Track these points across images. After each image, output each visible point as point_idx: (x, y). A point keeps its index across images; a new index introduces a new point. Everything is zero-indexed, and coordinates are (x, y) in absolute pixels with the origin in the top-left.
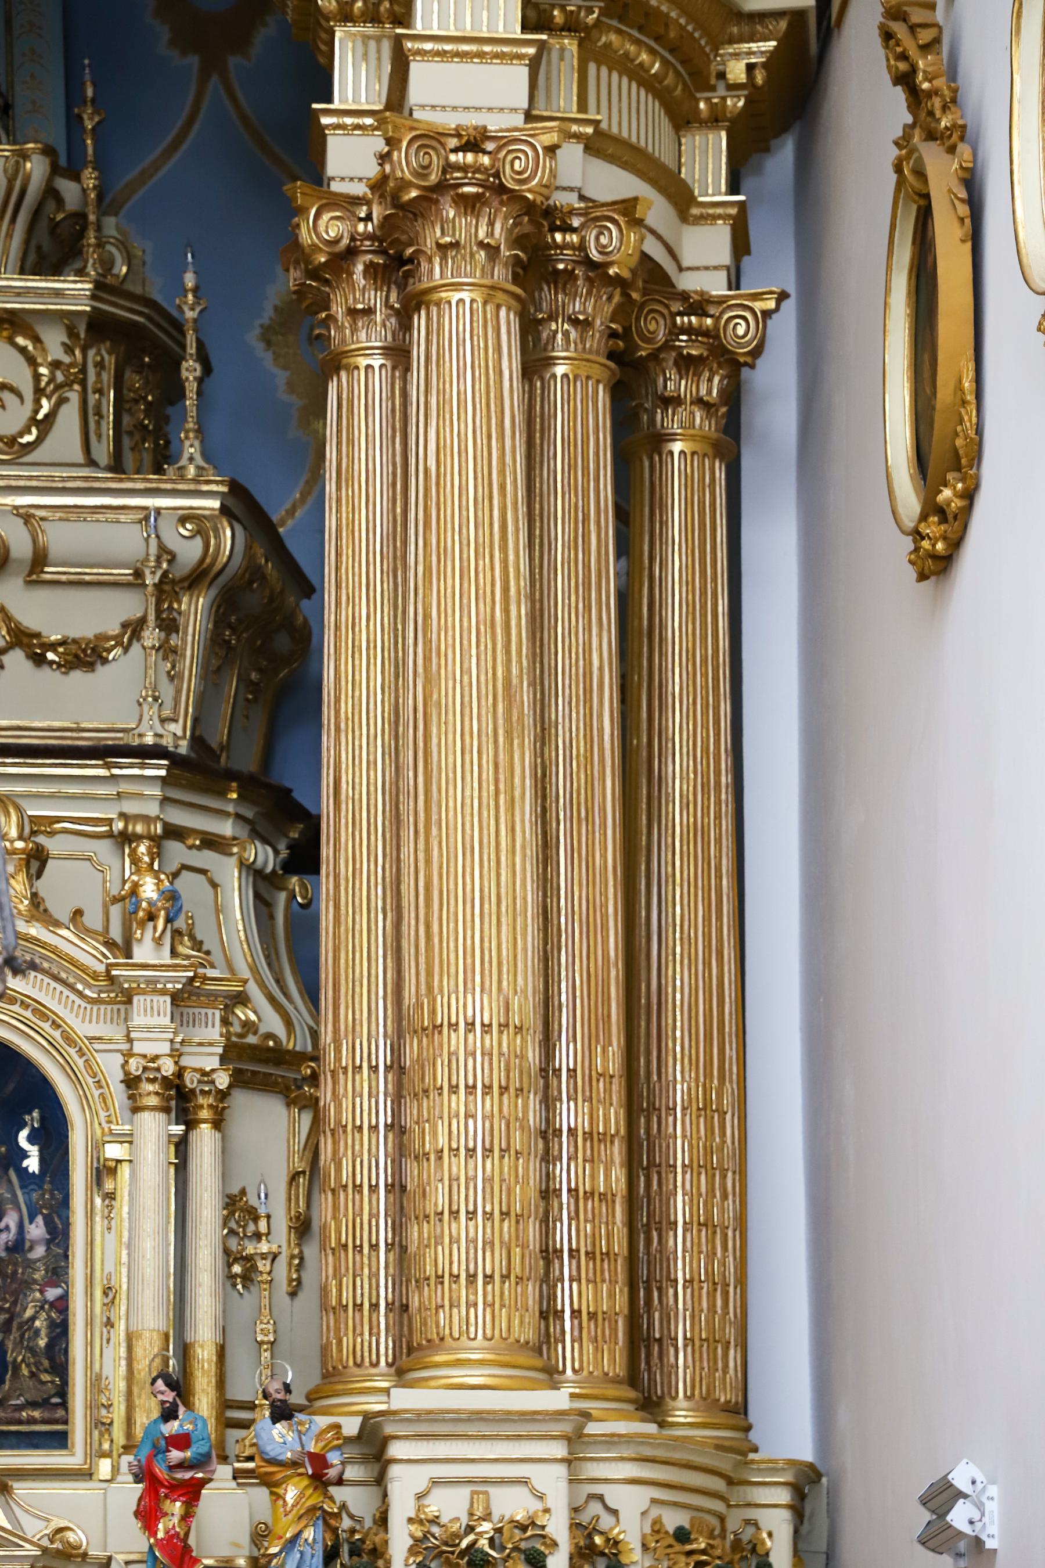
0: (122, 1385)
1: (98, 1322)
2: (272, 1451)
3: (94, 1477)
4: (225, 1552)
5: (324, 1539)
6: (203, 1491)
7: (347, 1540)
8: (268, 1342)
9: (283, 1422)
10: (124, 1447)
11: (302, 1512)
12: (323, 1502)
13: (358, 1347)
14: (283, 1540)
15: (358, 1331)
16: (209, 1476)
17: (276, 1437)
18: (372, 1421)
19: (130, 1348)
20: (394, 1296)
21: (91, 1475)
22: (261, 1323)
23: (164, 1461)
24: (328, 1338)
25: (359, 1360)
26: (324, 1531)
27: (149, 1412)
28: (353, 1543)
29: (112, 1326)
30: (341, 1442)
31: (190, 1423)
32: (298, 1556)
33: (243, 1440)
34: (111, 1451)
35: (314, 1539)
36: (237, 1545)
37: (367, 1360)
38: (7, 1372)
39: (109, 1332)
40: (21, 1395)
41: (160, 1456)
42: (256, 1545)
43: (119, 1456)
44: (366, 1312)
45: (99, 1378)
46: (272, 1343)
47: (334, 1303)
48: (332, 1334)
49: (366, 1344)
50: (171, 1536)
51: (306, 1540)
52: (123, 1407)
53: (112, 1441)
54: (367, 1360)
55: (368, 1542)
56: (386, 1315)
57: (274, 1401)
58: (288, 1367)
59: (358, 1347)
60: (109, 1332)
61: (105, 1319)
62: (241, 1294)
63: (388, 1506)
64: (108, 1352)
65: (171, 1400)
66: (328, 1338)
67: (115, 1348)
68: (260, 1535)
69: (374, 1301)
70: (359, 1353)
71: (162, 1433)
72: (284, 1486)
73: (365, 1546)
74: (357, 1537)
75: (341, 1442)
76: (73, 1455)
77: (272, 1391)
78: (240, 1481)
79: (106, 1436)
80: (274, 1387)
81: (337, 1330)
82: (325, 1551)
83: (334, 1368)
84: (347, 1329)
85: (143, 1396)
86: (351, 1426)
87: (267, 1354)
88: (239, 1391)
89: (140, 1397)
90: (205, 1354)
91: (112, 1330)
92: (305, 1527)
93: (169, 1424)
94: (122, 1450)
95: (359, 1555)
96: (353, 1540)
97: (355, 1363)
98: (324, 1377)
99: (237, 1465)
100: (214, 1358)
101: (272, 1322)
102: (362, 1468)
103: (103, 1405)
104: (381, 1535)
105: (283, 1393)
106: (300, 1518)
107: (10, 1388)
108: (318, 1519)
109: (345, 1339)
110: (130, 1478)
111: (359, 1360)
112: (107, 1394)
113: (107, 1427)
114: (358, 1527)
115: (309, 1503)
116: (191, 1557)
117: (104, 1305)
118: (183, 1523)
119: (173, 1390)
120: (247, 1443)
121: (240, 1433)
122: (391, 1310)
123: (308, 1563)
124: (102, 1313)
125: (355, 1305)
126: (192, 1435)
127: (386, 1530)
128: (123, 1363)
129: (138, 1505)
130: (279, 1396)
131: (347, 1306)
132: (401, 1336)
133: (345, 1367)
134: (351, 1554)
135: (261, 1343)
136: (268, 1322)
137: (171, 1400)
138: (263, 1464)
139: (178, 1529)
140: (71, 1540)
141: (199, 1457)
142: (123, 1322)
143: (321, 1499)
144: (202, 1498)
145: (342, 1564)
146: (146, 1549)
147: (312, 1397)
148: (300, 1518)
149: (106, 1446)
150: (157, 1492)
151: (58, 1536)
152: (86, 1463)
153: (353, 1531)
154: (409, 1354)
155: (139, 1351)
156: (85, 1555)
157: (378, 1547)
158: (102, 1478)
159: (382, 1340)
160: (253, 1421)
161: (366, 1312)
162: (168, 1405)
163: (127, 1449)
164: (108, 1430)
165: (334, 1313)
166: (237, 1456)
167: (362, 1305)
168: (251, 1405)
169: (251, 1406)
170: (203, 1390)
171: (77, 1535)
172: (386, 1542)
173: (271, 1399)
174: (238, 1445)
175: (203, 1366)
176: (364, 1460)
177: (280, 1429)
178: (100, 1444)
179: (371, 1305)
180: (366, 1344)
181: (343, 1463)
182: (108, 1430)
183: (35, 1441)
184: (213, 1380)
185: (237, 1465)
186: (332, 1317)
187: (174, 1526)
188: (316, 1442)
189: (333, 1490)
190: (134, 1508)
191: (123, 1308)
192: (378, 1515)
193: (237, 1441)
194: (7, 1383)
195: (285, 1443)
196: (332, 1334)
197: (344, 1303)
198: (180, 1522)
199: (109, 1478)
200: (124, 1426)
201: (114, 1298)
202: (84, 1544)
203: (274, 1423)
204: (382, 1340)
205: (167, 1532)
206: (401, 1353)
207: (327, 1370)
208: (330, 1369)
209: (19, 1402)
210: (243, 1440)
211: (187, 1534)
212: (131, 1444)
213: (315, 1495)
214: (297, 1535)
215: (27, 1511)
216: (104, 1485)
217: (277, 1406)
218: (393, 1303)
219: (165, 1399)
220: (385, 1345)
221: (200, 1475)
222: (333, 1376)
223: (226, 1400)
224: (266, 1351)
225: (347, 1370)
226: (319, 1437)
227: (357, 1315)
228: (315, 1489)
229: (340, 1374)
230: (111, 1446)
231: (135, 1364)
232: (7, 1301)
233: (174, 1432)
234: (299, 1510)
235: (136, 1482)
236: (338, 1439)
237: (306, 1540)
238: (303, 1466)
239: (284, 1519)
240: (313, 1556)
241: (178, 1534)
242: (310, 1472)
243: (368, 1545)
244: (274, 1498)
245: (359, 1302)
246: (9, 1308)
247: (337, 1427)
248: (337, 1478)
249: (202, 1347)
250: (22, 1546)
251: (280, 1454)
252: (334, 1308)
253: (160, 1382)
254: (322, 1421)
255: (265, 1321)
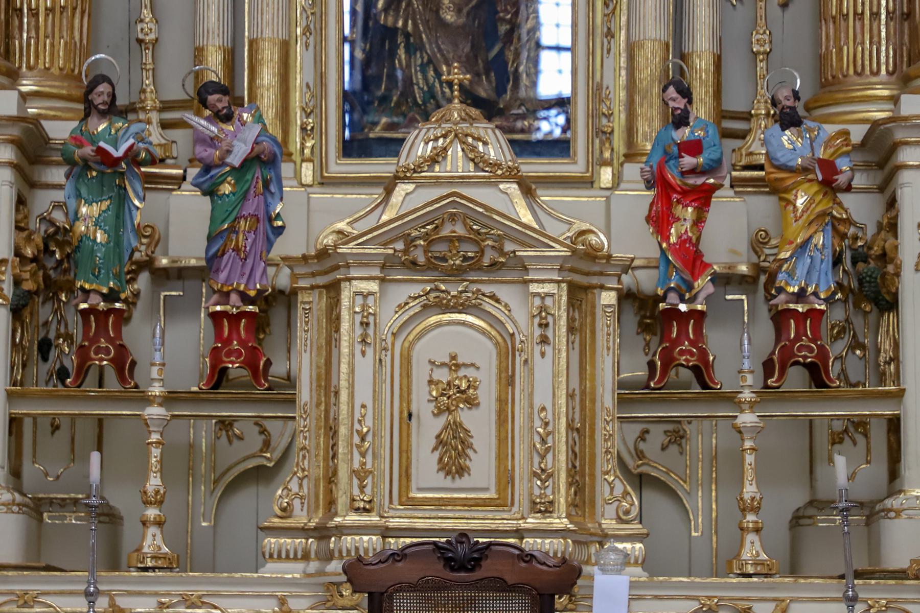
0: (623, 94)
1: (599, 31)
2: (782, 158)
3: (595, 185)
4: (726, 259)
5: (833, 245)
6: (713, 200)
7: (850, 247)
8: (764, 53)
9: (792, 128)
10: (625, 155)
11: (812, 217)
12: (832, 208)
13: (859, 56)
14: (794, 245)
15: (859, 40)
16: (720, 182)
17: (786, 143)
18: (882, 127)
19: (631, 58)
20: (894, 5)
21: (592, 183)
22: (757, 33)
23: (677, 168)
24: (827, 48)
25: (859, 69)
26: (833, 237)
27: (651, 121)
28: (856, 250)
29: (613, 37)
30: (850, 148)
31: (701, 130)
32: (809, 260)
33: (740, 149)
34: (612, 160)
35: (823, 244)
36: (734, 252)
37: (867, 68)
38: (508, 81)
39: (609, 43)
40: (522, 104)
41: (672, 162)
42: (756, 252)
43: (622, 165)
44: (867, 22)
45: (600, 87)
46: (768, 54)
47: (834, 13)
48: (832, 43)
49: (867, 53)
50: (683, 241)
51: (816, 245)
52: (623, 116)
53: (612, 150)
54: (867, 68)
55: (876, 248)
56: (887, 24)
57: (783, 108)
58: (796, 74)
59: (859, 56)
60: (609, 43)
61: (605, 30)
62: (734, 6)
63: (898, 211)
64: (609, 62)
65: (682, 107)
66: (827, 48)
67: (615, 58)
68: (758, 243)
69: (875, 10)
70: (859, 62)
71: (673, 139)
72: (794, 192)
73: (872, 252)
74: (860, 243)
75: (850, 148)
76: (575, 163)
77: (781, 98)
78: (737, 189)
79: (607, 145)
80: (783, 94)
81: (837, 39)
82: (834, 255)
83: (834, 77)
84: (848, 38)
85: (645, 106)
86: (857, 133)
87: (763, 65)
88: (734, 102)
89: (642, 106)
90: (702, 64)
91: (612, 41)
92: (815, 232)
93: (680, 130)
94: (622, 159)
95: (865, 261)
96: (856, 247)
97: (855, 72)
98: (823, 86)
99: (734, 173)
100: (712, 68)
101: (768, 32)
102: (865, 175)
103: (604, 114)
104: (891, 241)
105: (792, 100)
106: (810, 224)
107: (511, 98)
108: (827, 224)
109: (845, 48)
110: (643, 186)
111: (859, 69)
112: (608, 103)
113: (606, 135)
114: (860, 235)
115: (819, 209)
116: (702, 262)
117: (605, 15)
118: (695, 228)
119: (684, 97)
120: (744, 153)
121: (737, 143)
122: (892, 19)
123: (817, 268)
124: (602, 23)
125: (855, 13)
126: (704, 141)
127: (896, 236)
128: (623, 73)
129: (650, 211)
130: (788, 103)
131: (848, 14)
132: (902, 44)
133: (845, 76)
134: (854, 262)
135: (756, 54)
136: (764, 32)
137: (682, 107)
138: (772, 170)
139: (690, 234)
140: (594, 242)
141: (711, 163)
142: (623, 33)
143: (831, 205)
144: (712, 204)
145: (844, 270)
146: (657, 254)
147: (811, 106)
148: (810, 224)
149: (607, 155)
150: (669, 198)
151: (580, 239)
152: (588, 171)
153: (856, 238)
154: (909, 65)
155: (640, 61)
156: (609, 257)
157: (888, 251)
158: (602, 186)
159: (883, 48)
160: (749, 131)
161: (867, 22)
162: (679, 112)
163: (630, 157)
164: (608, 139)
165: (834, 22)
166: (734, 165)
167: (863, 13)
168: (745, 116)
169: (747, 117)
170: (701, 100)
171: (599, 237)
172: (896, 247)
173: (780, 106)
174: (734, 155)
175: (701, 77)
176: (867, 166)
177: (787, 137)
178: (601, 152)
179: (872, 14)
180: (867, 53)
181: (851, 169)
182: (608, 139)
183: (538, 150)
184: (711, 90)
185: (734, 173)
186: (831, 26)
187: (686, 231)
188: (825, 149)
189: (843, 198)
190: (647, 213)
191: (624, 19)
192: (885, 221)
193: (734, 150)
194: (508, 93)
195: (794, 149)
196: (832, 43)
197: (845, 11)
198: (692, 227)
199: (609, 185)
200: (625, 135)
201: (615, 8)
202: (606, 246)
203: (783, 130)
204: (883, 48)
205: (679, 237)
206: (902, 62)
207: (826, 79)
208: (830, 78)
209: (520, 111)
210: (740, 149)
211: (698, 239)
212: (632, 152)
213: (825, 201)
214: (808, 240)
215: (549, 214)
216: (607, 193)
217: (785, 113)
218: (894, 12)
219: (677, 106)
220: (886, 52)
221: (712, 181)
222: (832, 84)
223: (722, 111)
224: (761, 61)
225: (847, 79)
226: (827, 144)
227: (858, 24)
228: (825, 194)
229: (840, 83)
230: (612, 154)
231: (637, 74)
232: (509, 13)
233: (685, 138)
234: (809, 216)
235: (648, 188)
236: (847, 145)
237: (816, 245)
238: (813, 172)
239: (794, 224)
240: (822, 261)
241: (690, 239)
242: (820, 178)
243: (876, 250)
244: (784, 204)
245: (860, 10)
246: (511, 19)
247: (846, 133)
248: (847, 183)
249: (700, 57)
250: (553, 247)
251: (790, 161)
252: (834, 18)
253: (671, 89)
254: (830, 129)
255: (761, 32)
